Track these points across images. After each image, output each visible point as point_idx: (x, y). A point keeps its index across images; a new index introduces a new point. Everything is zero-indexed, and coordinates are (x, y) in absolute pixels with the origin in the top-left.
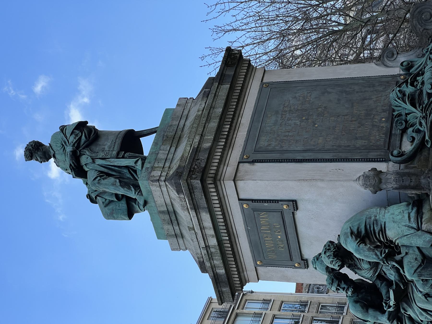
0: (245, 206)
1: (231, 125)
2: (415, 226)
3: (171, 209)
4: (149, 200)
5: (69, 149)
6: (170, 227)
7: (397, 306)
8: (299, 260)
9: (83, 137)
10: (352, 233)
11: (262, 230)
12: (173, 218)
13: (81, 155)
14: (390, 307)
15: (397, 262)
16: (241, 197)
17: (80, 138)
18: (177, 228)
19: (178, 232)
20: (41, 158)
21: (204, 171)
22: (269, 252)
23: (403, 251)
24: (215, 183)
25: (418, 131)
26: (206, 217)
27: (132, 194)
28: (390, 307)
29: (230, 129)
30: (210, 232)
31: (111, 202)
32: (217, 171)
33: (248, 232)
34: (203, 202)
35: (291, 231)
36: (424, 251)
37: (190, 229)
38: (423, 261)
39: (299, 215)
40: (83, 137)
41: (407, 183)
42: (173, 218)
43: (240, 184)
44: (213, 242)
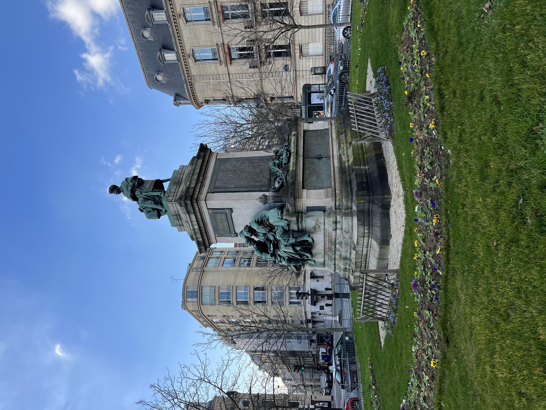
1: (203, 177)
2: (280, 217)
3: (177, 213)
4: (168, 210)
5: (130, 188)
6: (177, 221)
7: (274, 251)
8: (234, 233)
9: (136, 183)
10: (255, 221)
12: (179, 217)
13: (135, 191)
14: (271, 251)
15: (273, 233)
17: (135, 184)
19: (181, 223)
21: (192, 197)
23: (276, 228)
24: (197, 202)
25: (281, 179)
26: (193, 217)
27: (159, 207)
28: (271, 251)
29: (203, 178)
31: (150, 211)
32: (198, 197)
33: (212, 222)
34: (192, 210)
35: (230, 221)
36: (284, 228)
37: (186, 222)
38: (284, 232)
39: (233, 214)
40: (136, 183)
41: (277, 200)
42: (179, 217)
43: (208, 202)
44: (196, 227)
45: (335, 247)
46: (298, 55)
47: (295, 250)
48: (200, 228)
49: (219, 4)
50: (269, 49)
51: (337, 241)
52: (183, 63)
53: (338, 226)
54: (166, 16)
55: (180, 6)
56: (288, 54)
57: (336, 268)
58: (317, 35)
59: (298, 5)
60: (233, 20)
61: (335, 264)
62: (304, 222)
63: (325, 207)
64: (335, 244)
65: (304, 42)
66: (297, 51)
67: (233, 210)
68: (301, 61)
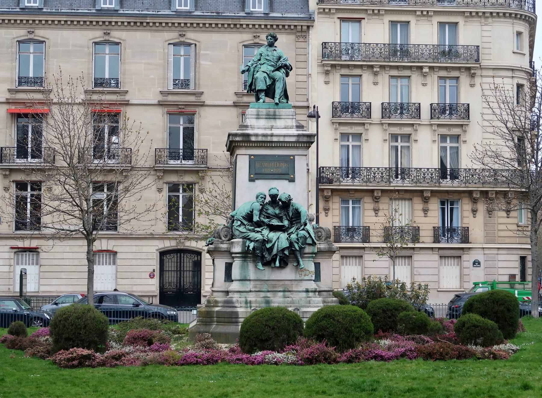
0: (292, 157)
3: (277, 117)
8: (255, 177)
11: (276, 163)
12: (271, 117)
13: (284, 69)
16: (296, 156)
18: (264, 117)
20: (272, 42)
22: (261, 164)
26: (293, 139)
30: (282, 139)
33: (274, 156)
37: (272, 126)
42: (271, 117)
44: (275, 139)
45: (280, 291)
46: (20, 244)
47: (283, 250)
48: (272, 142)
49: (122, 109)
50: (32, 189)
51: (287, 293)
52: (19, 18)
53: (311, 294)
54: (108, 10)
55: (123, 38)
56: (20, 225)
57: (242, 294)
58: (54, 282)
59: (110, 248)
60: (91, 131)
61: (250, 291)
62: (311, 259)
63: (320, 281)
64: (284, 291)
65: (42, 255)
66: (27, 244)
67: (292, 184)
68: (7, 249)
